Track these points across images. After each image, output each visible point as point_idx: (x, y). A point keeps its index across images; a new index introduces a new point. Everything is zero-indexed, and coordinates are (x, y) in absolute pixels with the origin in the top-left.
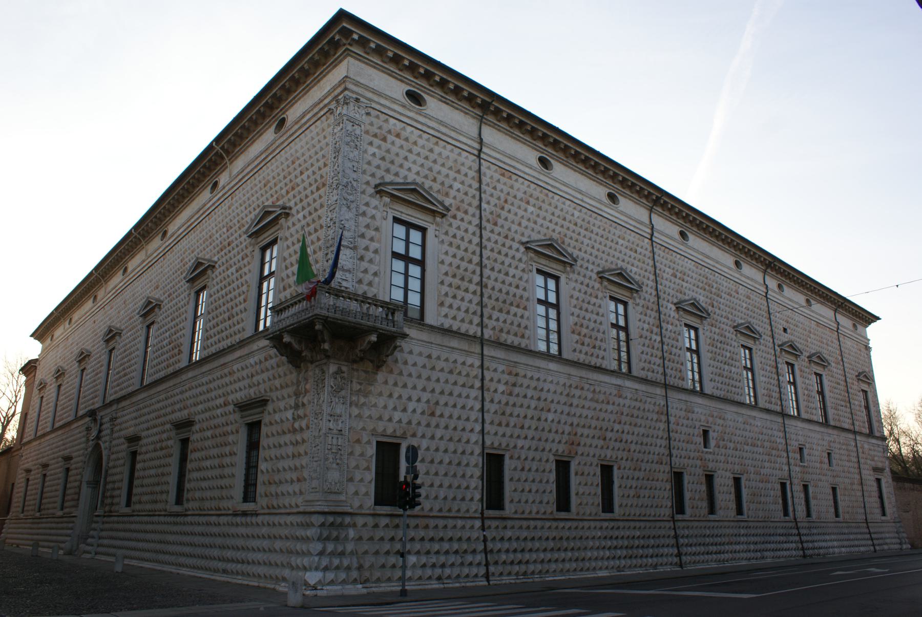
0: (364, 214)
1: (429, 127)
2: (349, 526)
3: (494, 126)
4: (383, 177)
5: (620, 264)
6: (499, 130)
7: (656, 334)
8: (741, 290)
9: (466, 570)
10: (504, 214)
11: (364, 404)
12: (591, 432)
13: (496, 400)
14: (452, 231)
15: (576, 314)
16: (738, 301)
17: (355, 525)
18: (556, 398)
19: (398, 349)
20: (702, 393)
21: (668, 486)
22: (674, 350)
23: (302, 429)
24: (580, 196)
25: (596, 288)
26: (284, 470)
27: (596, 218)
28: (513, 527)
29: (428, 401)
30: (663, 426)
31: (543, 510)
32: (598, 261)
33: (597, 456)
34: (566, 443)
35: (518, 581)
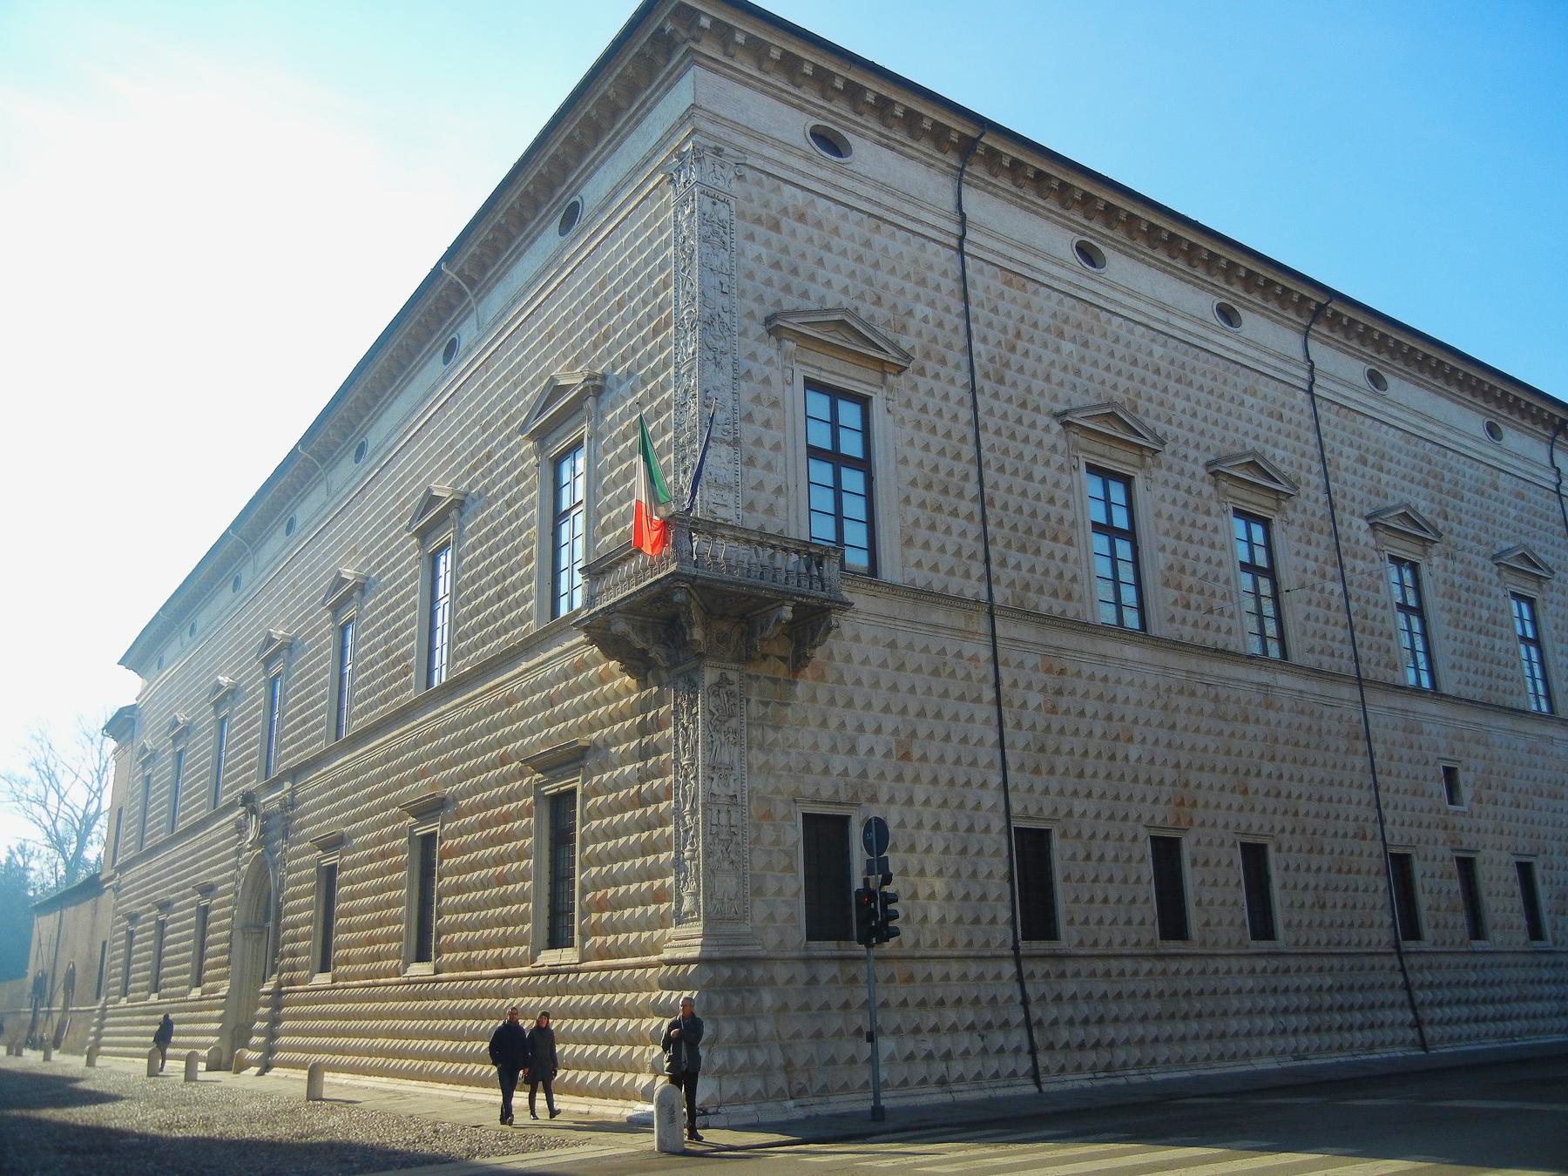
3: (985, 187)
4: (778, 302)
5: (1251, 444)
6: (996, 195)
7: (1333, 579)
9: (993, 1064)
10: (1015, 359)
13: (1026, 724)
14: (919, 398)
17: (772, 981)
19: (833, 632)
20: (1435, 692)
21: (1382, 884)
22: (1371, 610)
24: (1161, 315)
27: (1196, 357)
28: (1077, 974)
30: (1360, 762)
33: (1232, 826)
35: (1097, 1083)
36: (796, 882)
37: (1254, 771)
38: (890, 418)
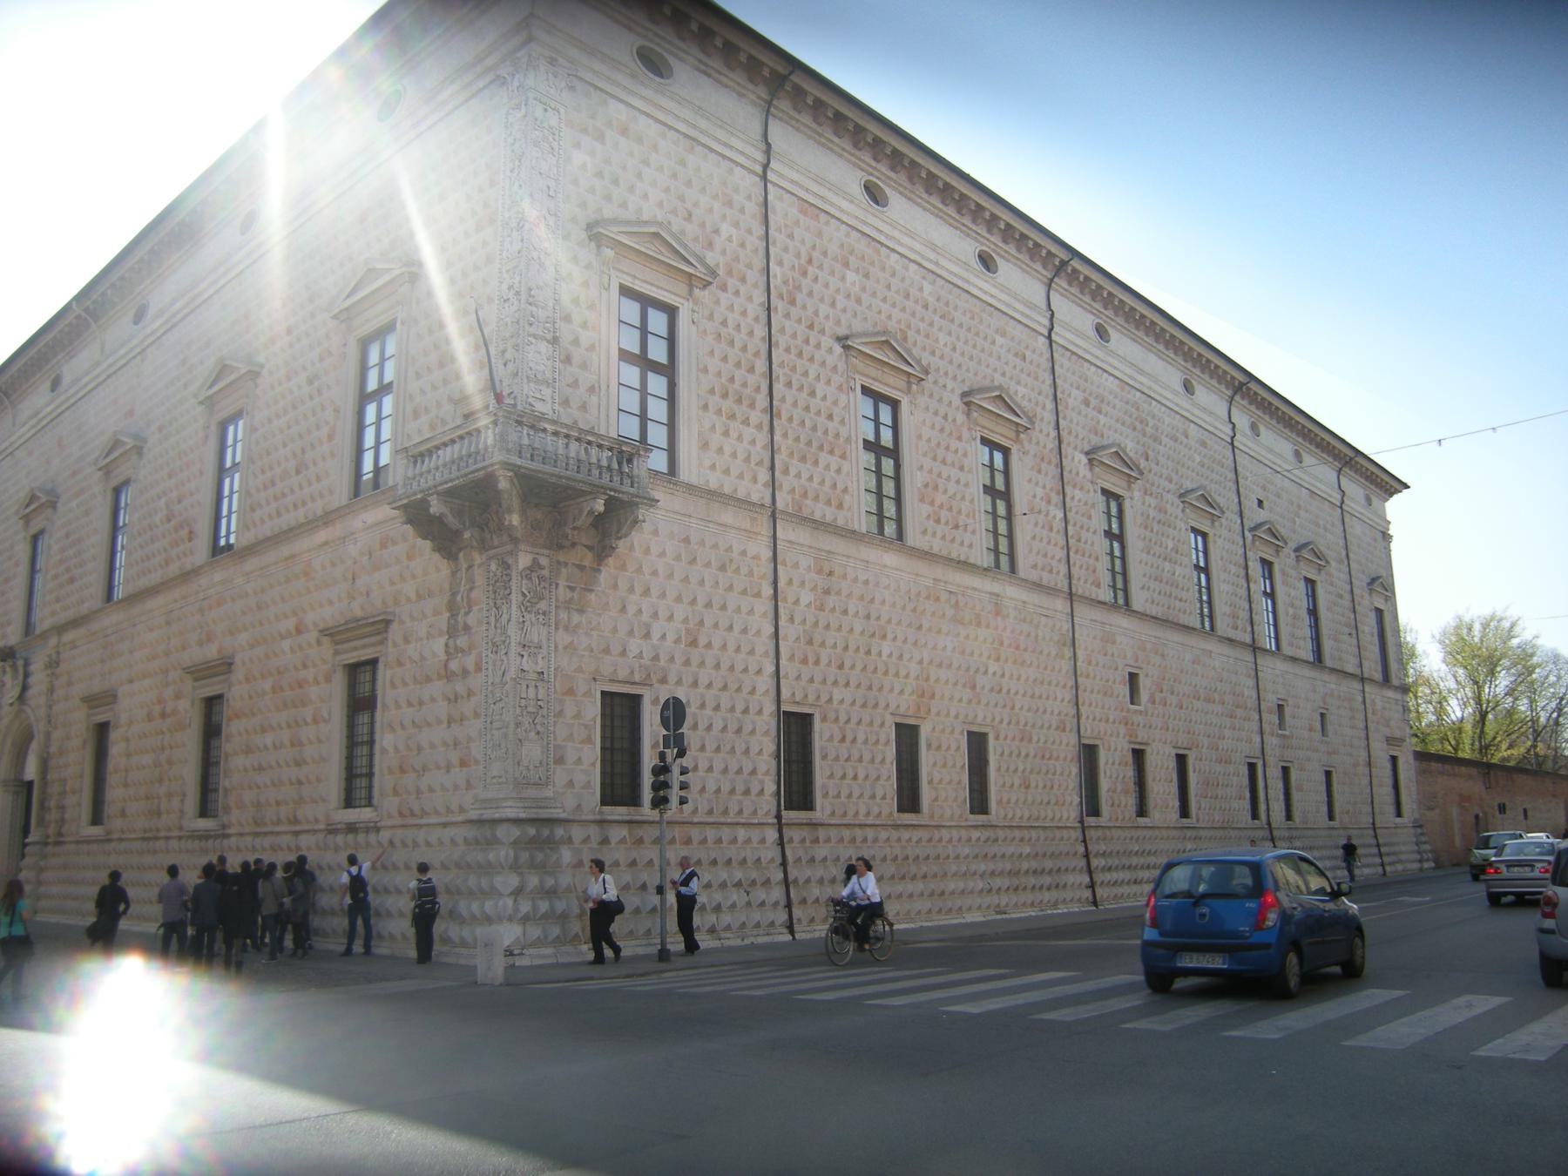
5: (998, 380)
6: (798, 129)
13: (798, 619)
17: (570, 841)
21: (1075, 770)
23: (465, 672)
24: (933, 256)
28: (828, 840)
30: (1066, 666)
31: (876, 810)
36: (592, 754)
37: (982, 669)
38: (694, 328)
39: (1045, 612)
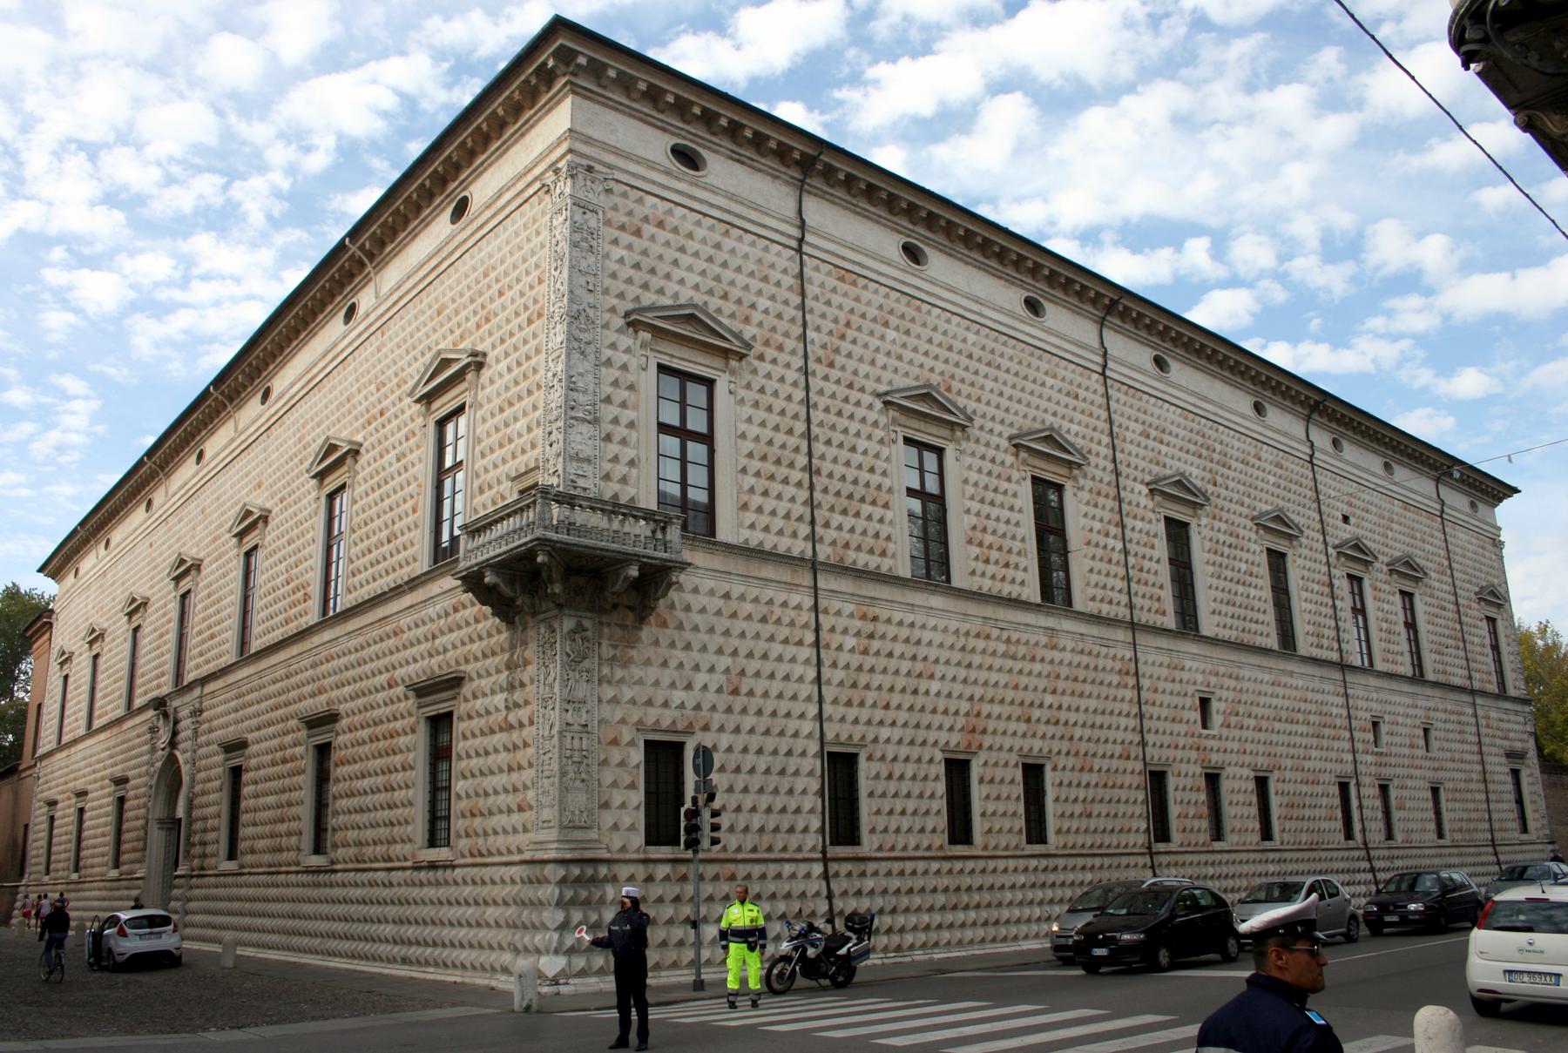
0: (609, 363)
1: (712, 205)
2: (606, 880)
3: (822, 195)
4: (637, 299)
5: (1049, 419)
6: (833, 202)
7: (1115, 537)
8: (1266, 453)
10: (846, 346)
11: (621, 681)
12: (1006, 710)
13: (841, 664)
14: (759, 381)
15: (974, 511)
16: (1260, 473)
18: (945, 655)
21: (1141, 796)
23: (521, 725)
24: (975, 307)
25: (1008, 463)
26: (496, 792)
27: (1005, 344)
28: (876, 874)
29: (727, 671)
30: (1129, 694)
32: (1009, 418)
34: (962, 729)
39: (1105, 642)
